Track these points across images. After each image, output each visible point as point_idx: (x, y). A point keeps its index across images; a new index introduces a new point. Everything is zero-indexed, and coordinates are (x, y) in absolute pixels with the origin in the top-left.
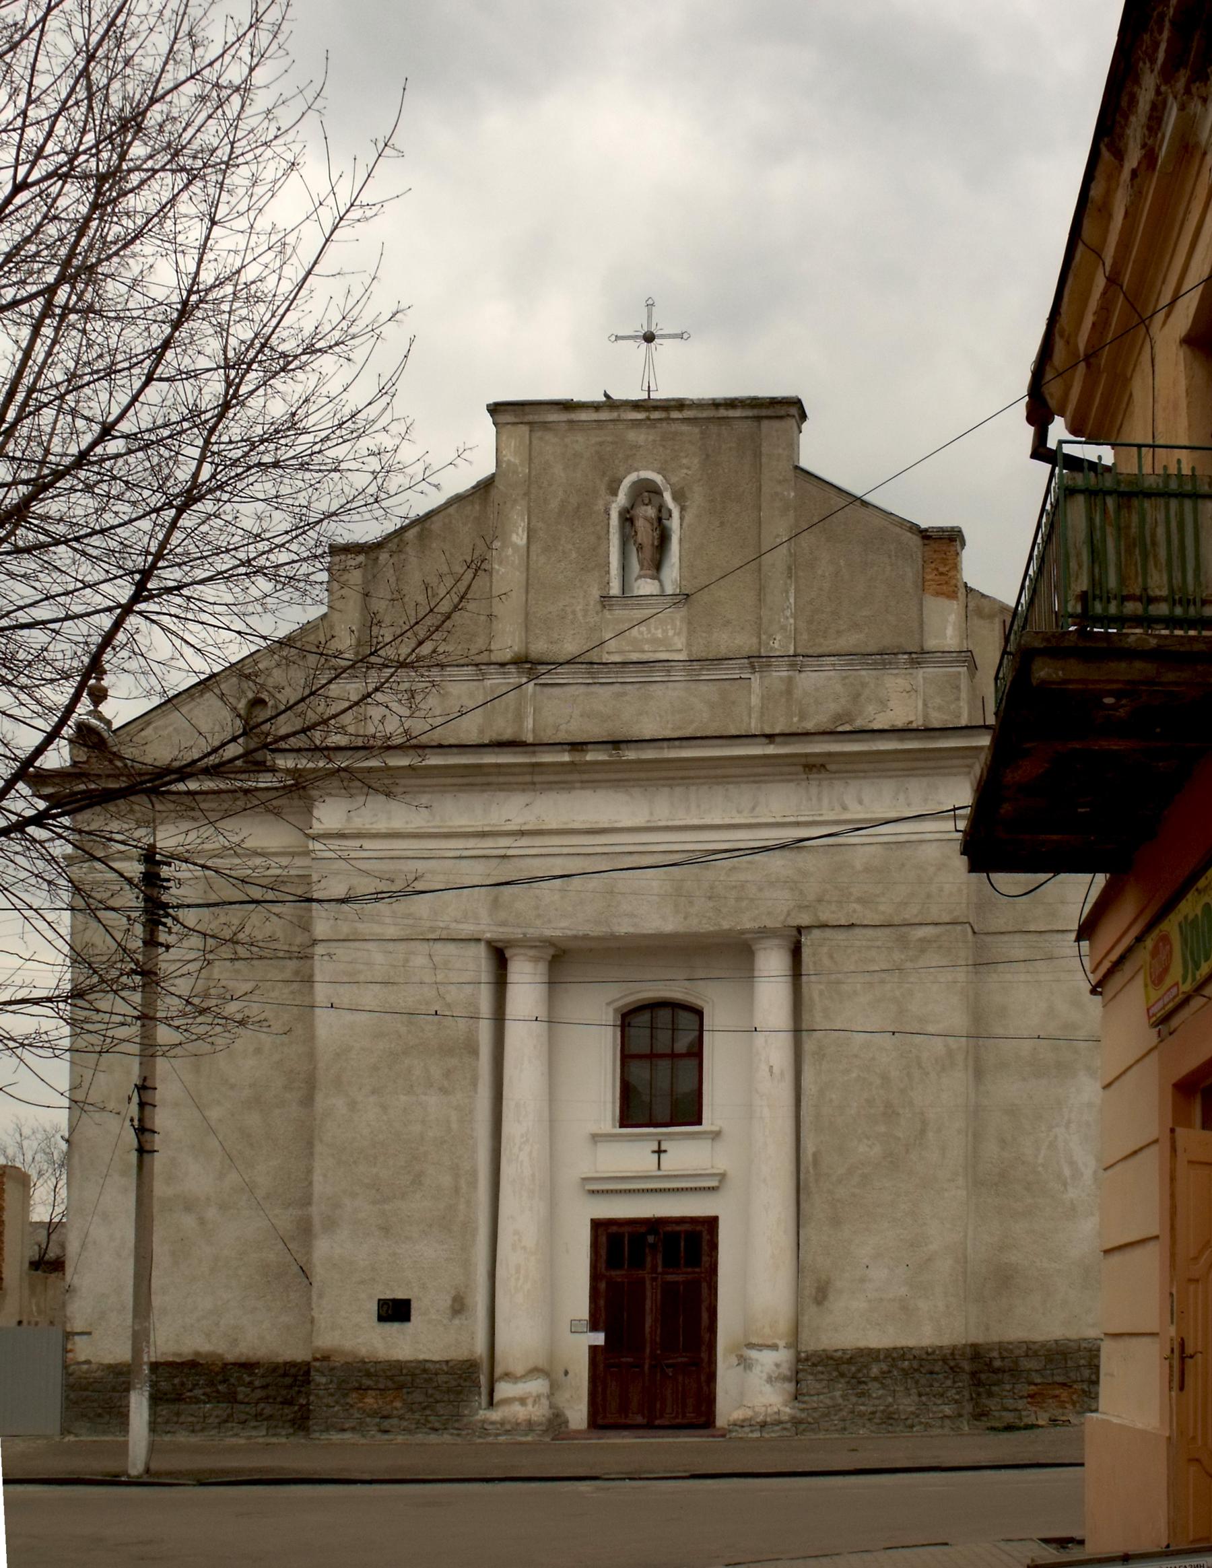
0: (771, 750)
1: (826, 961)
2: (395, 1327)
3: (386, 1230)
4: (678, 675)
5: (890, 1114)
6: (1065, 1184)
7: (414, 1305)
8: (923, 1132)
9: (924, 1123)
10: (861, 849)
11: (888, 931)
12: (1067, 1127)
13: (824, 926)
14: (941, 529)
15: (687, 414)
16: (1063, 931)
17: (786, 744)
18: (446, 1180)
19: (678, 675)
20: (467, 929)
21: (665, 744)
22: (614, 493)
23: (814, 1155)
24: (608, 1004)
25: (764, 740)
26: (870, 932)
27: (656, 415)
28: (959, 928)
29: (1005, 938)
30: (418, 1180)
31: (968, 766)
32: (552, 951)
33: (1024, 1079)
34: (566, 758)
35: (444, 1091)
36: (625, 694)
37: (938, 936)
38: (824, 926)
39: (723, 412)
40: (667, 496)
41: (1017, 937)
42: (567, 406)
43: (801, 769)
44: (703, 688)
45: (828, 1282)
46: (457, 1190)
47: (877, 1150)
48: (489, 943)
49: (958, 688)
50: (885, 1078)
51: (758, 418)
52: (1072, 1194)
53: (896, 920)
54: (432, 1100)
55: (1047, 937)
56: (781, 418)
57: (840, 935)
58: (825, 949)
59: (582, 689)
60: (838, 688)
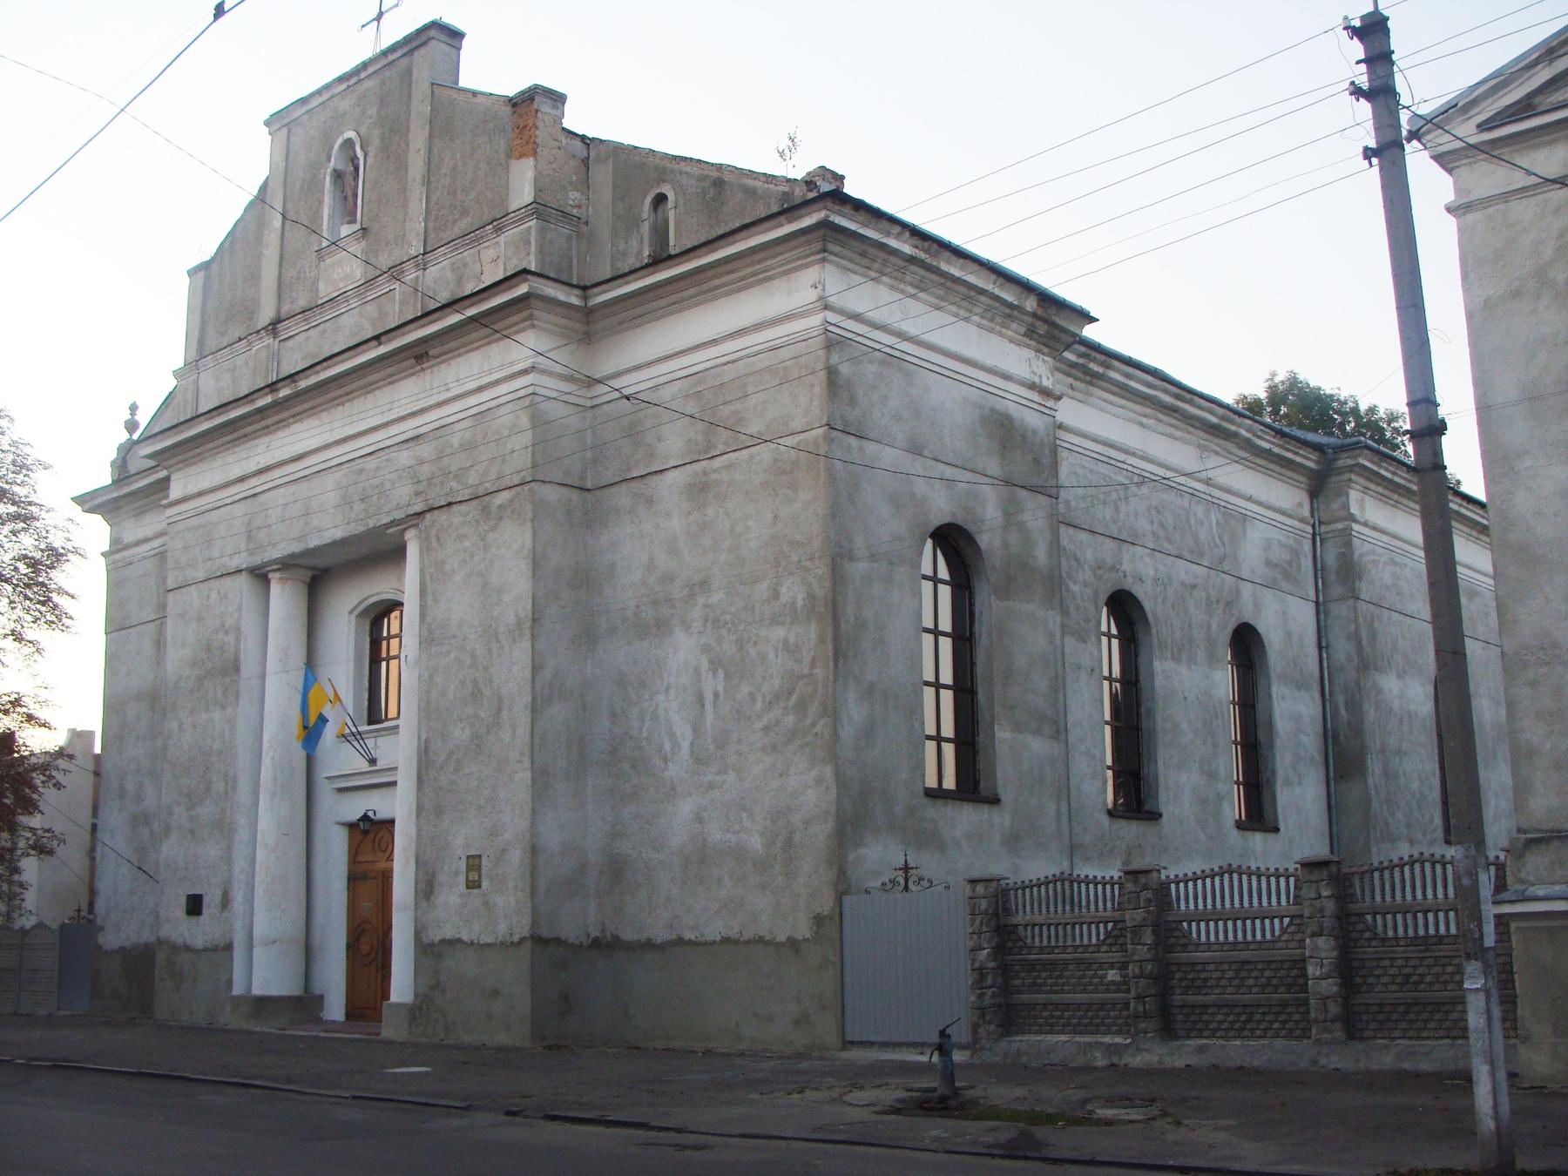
0: (383, 350)
1: (435, 544)
2: (194, 919)
3: (192, 832)
4: (354, 303)
5: (476, 695)
6: (666, 761)
7: (205, 900)
8: (499, 709)
9: (500, 701)
10: (457, 427)
11: (475, 503)
12: (667, 691)
13: (431, 509)
14: (522, 93)
15: (371, 70)
16: (661, 471)
17: (390, 341)
18: (221, 786)
19: (354, 303)
20: (235, 563)
21: (318, 368)
22: (329, 160)
23: (426, 741)
24: (351, 612)
25: (374, 343)
26: (463, 507)
27: (353, 81)
28: (526, 487)
29: (614, 490)
30: (208, 790)
31: (527, 319)
32: (310, 574)
33: (630, 643)
34: (269, 399)
35: (223, 707)
36: (324, 332)
37: (511, 501)
38: (431, 509)
39: (391, 58)
40: (358, 148)
41: (624, 486)
42: (303, 101)
43: (413, 361)
44: (369, 307)
45: (434, 875)
46: (226, 792)
47: (467, 732)
48: (246, 569)
49: (529, 242)
50: (473, 656)
51: (411, 51)
52: (673, 771)
53: (481, 491)
54: (217, 715)
55: (648, 480)
56: (424, 43)
57: (441, 517)
58: (434, 532)
59: (303, 335)
60: (449, 275)
